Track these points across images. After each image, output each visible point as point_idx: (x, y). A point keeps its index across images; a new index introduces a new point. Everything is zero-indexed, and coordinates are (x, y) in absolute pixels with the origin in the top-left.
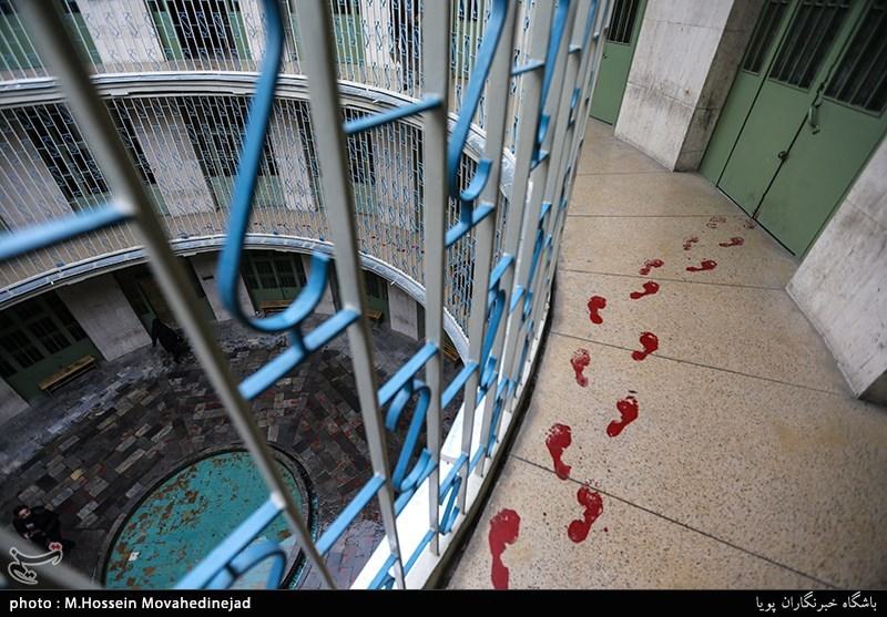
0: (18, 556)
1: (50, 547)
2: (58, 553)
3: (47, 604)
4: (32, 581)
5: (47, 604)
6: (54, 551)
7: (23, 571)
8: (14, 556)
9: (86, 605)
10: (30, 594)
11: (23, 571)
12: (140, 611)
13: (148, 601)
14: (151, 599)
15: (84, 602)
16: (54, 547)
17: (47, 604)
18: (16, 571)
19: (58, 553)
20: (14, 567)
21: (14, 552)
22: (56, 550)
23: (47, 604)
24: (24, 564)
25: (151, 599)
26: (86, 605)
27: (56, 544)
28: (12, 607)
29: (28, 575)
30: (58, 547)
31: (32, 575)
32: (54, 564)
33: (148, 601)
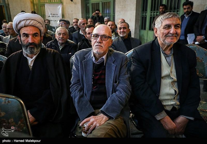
0: (4, 130)
1: (11, 128)
2: (13, 129)
3: (10, 141)
4: (7, 136)
5: (9, 141)
6: (12, 129)
7: (5, 133)
8: (3, 130)
9: (15, 141)
10: (6, 138)
11: (5, 133)
12: (25, 142)
13: (27, 140)
14: (28, 140)
15: (14, 141)
16: (12, 128)
17: (9, 141)
18: (3, 133)
19: (13, 129)
20: (3, 132)
21: (3, 129)
22: (13, 128)
23: (10, 141)
24: (4, 131)
25: (28, 140)
26: (15, 141)
27: (13, 127)
28: (3, 142)
29: (6, 134)
30: (13, 128)
31: (7, 134)
32: (12, 132)
33: (27, 140)
